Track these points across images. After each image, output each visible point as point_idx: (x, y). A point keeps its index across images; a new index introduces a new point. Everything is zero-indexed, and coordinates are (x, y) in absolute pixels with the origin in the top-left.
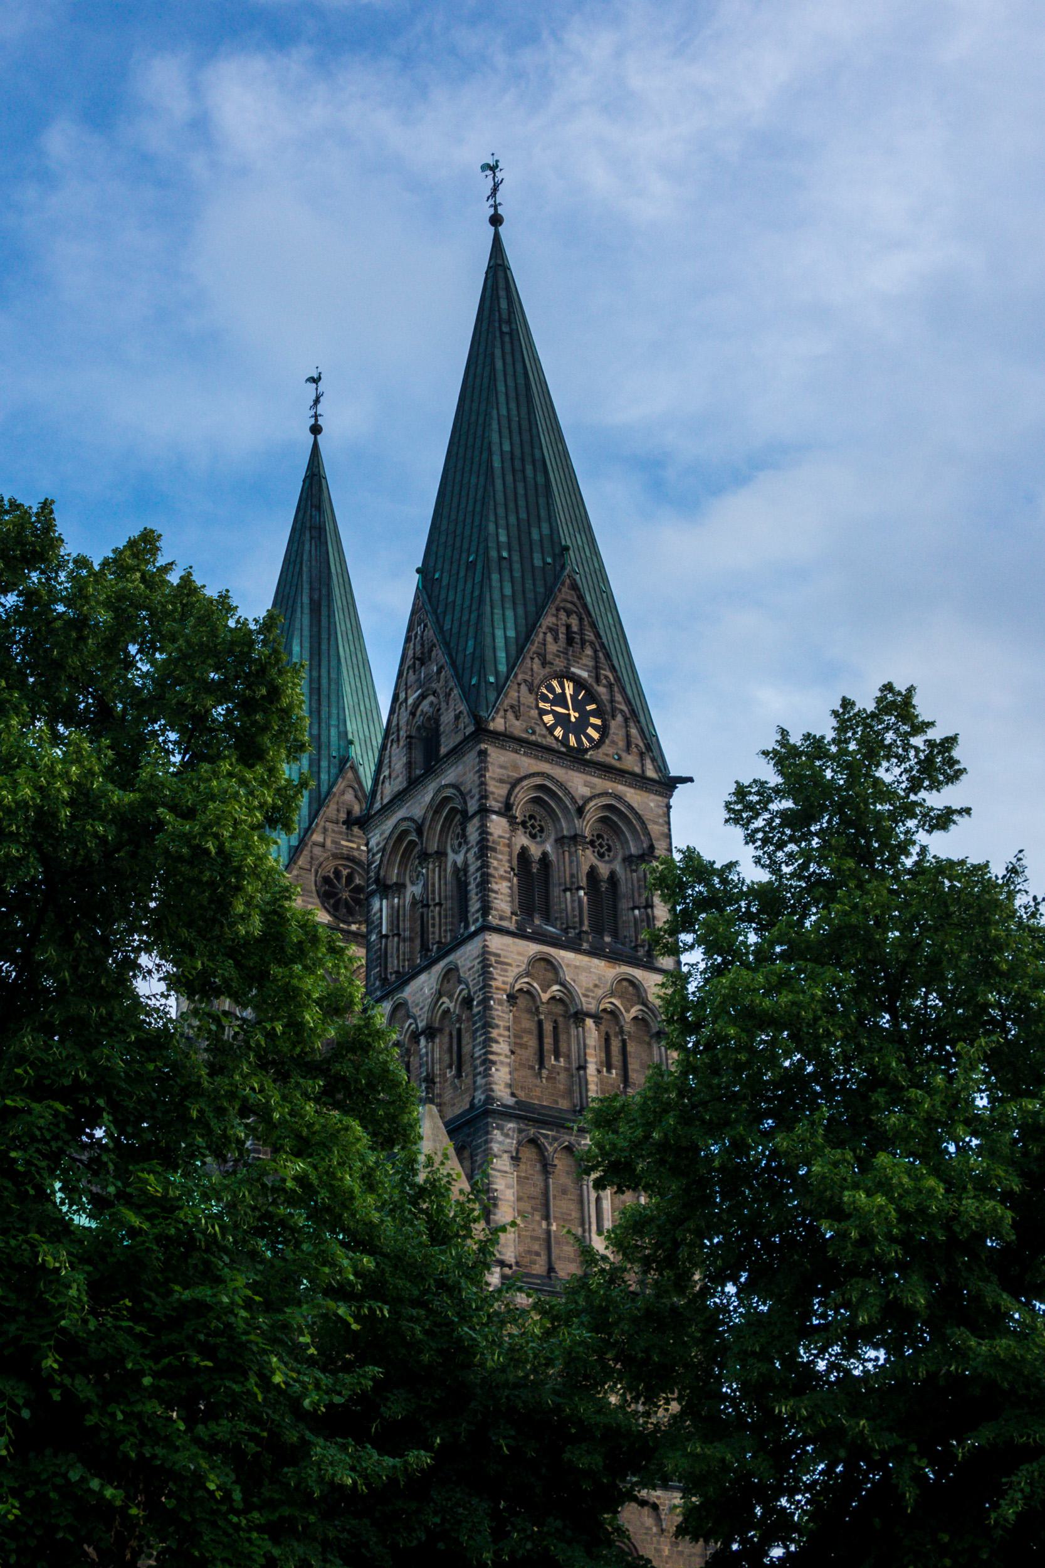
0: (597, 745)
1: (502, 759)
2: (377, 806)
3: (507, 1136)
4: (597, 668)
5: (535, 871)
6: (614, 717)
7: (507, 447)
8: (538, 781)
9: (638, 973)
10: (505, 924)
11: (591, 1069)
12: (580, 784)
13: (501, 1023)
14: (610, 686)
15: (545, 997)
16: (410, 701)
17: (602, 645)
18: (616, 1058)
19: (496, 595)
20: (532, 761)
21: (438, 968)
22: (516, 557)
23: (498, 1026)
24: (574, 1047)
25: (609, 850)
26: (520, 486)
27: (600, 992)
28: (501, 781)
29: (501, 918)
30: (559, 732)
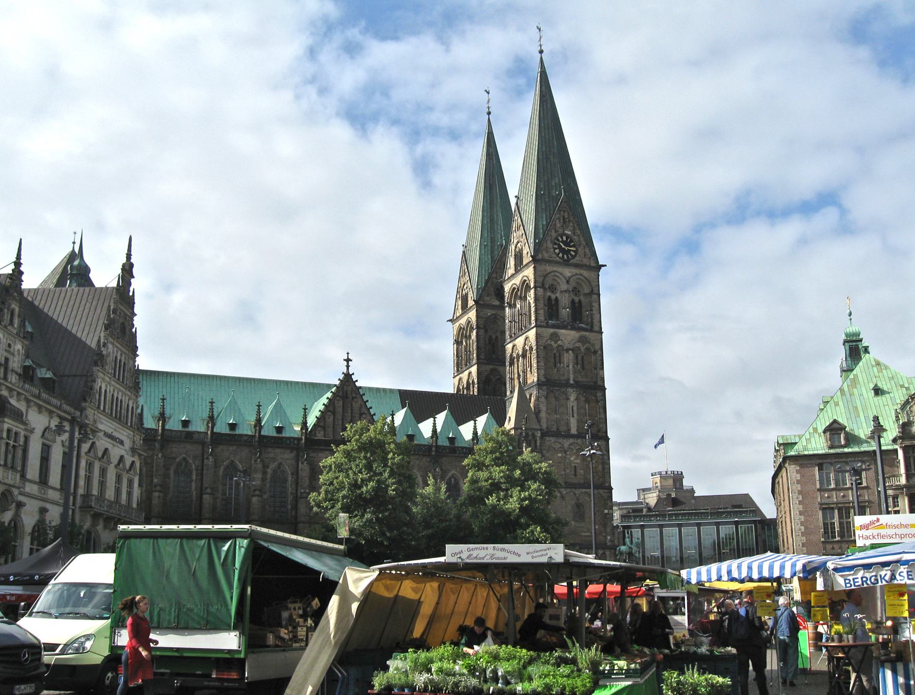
0: (574, 257)
2: (507, 278)
3: (543, 391)
4: (574, 230)
6: (580, 246)
11: (571, 367)
15: (556, 345)
16: (515, 243)
18: (580, 362)
21: (524, 336)
22: (547, 193)
25: (579, 292)
27: (574, 342)
28: (541, 276)
29: (541, 322)
30: (561, 255)
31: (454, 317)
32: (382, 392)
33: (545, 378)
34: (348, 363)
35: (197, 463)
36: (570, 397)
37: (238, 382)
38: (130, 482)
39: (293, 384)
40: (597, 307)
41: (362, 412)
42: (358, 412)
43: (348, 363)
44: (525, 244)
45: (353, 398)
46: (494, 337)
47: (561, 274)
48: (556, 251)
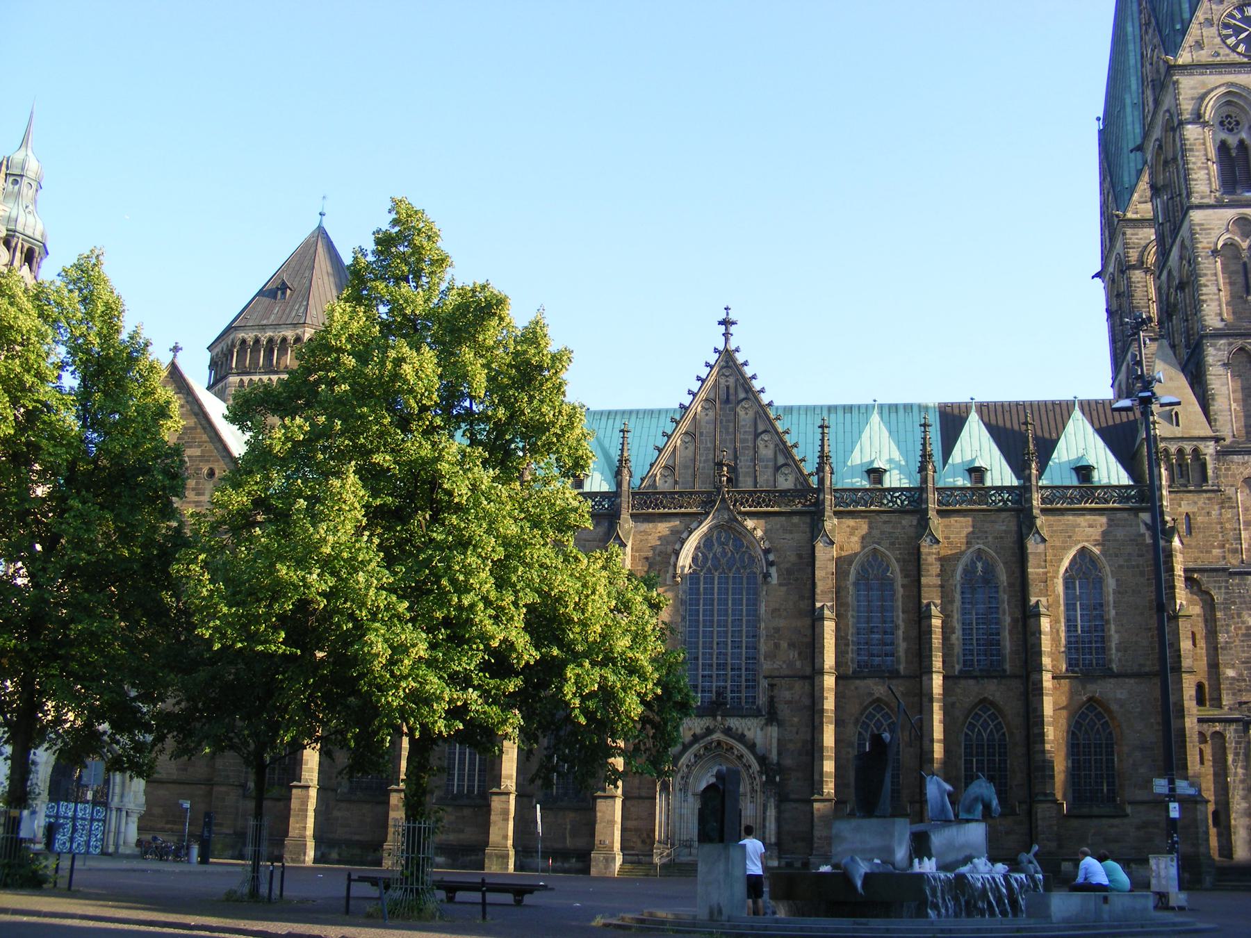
1: (1192, 82)
3: (1219, 350)
5: (1234, 155)
8: (1223, 90)
10: (1206, 201)
13: (1209, 272)
23: (1206, 275)
29: (1202, 198)
41: (761, 428)
42: (752, 430)
45: (739, 402)
48: (1229, 41)
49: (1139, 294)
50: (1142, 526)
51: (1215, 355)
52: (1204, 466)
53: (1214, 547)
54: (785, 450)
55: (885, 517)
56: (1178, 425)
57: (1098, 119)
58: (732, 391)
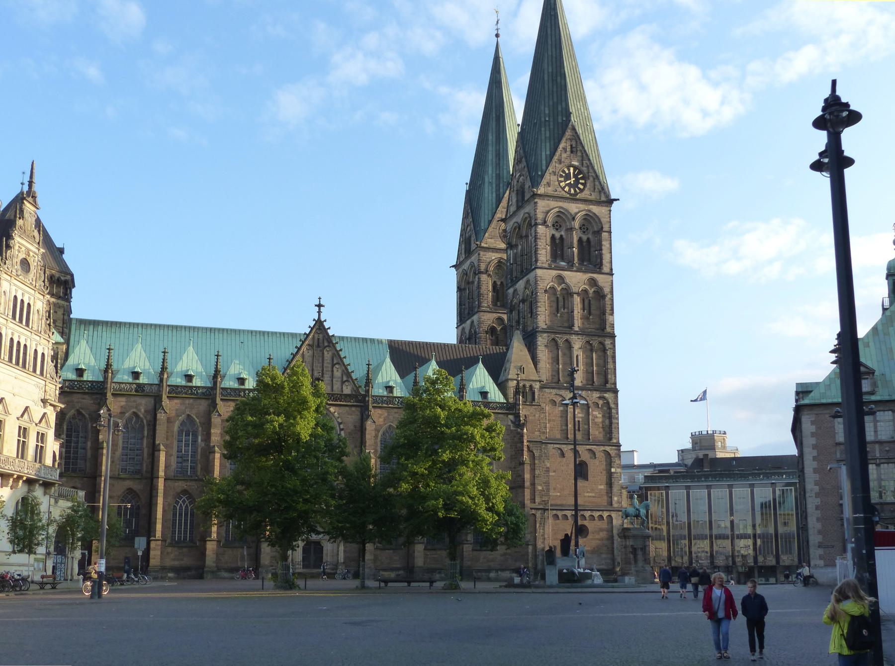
0: (582, 191)
1: (543, 204)
2: (508, 215)
3: (543, 338)
7: (550, 70)
8: (557, 210)
9: (595, 276)
12: (573, 208)
14: (588, 167)
16: (517, 177)
17: (585, 151)
19: (543, 138)
20: (555, 202)
21: (525, 279)
22: (551, 120)
23: (540, 302)
24: (570, 305)
26: (555, 87)
30: (567, 189)
31: (457, 262)
32: (369, 342)
33: (546, 324)
34: (319, 309)
35: (149, 417)
36: (574, 345)
37: (208, 333)
38: (41, 437)
39: (270, 335)
40: (608, 246)
42: (331, 362)
43: (319, 309)
44: (527, 178)
46: (499, 283)
47: (566, 210)
48: (561, 184)
49: (484, 287)
50: (509, 421)
51: (542, 341)
52: (533, 394)
53: (536, 431)
54: (348, 374)
55: (395, 410)
56: (524, 373)
57: (467, 184)
58: (321, 341)
